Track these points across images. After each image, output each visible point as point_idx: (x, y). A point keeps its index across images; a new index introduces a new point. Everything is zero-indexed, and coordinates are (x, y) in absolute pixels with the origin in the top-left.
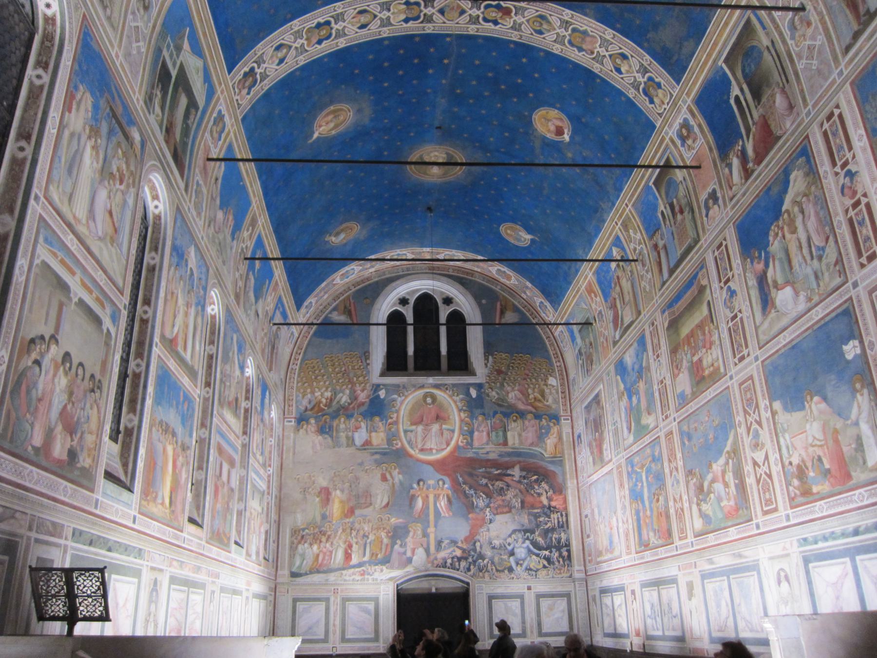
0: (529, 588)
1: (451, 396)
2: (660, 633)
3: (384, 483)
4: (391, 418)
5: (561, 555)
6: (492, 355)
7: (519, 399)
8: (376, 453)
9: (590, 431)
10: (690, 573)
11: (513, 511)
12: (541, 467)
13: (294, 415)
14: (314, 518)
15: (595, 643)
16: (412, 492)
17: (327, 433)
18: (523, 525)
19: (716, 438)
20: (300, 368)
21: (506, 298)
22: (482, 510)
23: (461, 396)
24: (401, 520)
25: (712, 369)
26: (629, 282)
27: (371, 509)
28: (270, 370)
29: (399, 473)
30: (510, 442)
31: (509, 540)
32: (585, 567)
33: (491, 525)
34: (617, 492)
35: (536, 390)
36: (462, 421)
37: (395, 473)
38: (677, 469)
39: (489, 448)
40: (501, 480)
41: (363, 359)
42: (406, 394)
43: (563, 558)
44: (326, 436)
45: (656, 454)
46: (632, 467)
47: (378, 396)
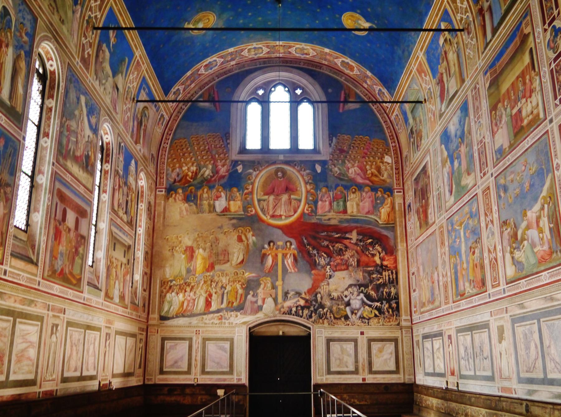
0: (362, 333)
1: (299, 171)
2: (472, 373)
3: (240, 244)
4: (248, 189)
5: (390, 306)
6: (336, 137)
7: (358, 174)
8: (234, 218)
9: (418, 199)
10: (501, 318)
11: (350, 268)
12: (376, 232)
13: (164, 186)
14: (180, 272)
15: (418, 382)
16: (263, 251)
17: (192, 201)
18: (358, 281)
19: (532, 186)
20: (170, 146)
21: (349, 88)
22: (323, 267)
23: (308, 171)
24: (253, 275)
25: (531, 117)
26: (455, 55)
27: (228, 265)
28: (137, 142)
29: (253, 235)
30: (349, 211)
31: (346, 293)
32: (411, 316)
33: (331, 280)
34: (439, 249)
35: (373, 167)
36: (308, 192)
37: (250, 235)
38: (492, 222)
39: (331, 215)
40: (341, 243)
41: (224, 139)
42: (260, 169)
43: (392, 309)
44: (192, 204)
45: (474, 210)
46: (452, 225)
47: (237, 170)
